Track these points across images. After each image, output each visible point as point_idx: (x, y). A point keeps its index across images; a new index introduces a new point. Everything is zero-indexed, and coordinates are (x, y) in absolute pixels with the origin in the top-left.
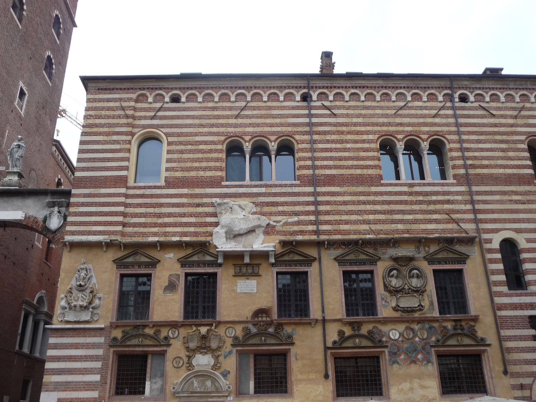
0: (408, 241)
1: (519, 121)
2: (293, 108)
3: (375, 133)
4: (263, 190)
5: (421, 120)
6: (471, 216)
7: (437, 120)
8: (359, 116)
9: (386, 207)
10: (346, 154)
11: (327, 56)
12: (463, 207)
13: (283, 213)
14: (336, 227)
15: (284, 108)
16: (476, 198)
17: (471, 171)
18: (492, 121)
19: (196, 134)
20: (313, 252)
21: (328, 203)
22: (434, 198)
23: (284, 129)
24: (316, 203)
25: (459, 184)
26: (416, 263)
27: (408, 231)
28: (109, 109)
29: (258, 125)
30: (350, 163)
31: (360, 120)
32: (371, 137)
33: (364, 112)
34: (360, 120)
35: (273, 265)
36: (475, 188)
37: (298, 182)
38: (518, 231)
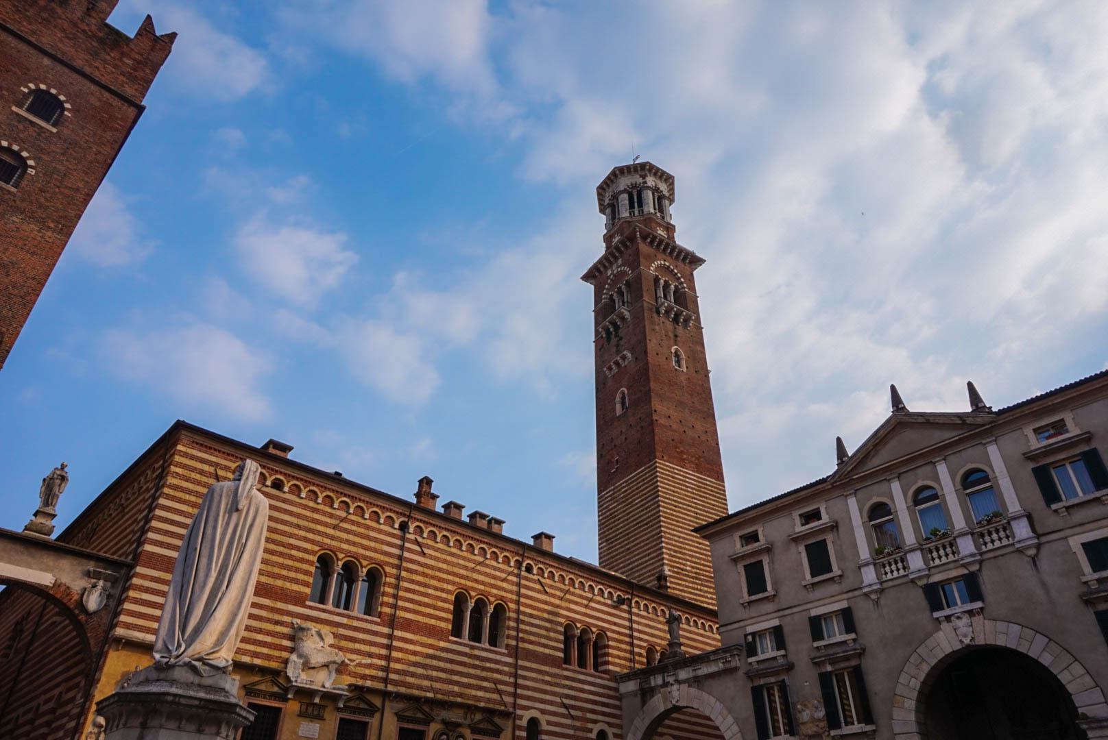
0: (460, 705)
1: (564, 604)
2: (390, 535)
3: (453, 583)
4: (345, 621)
5: (493, 581)
6: (511, 689)
7: (505, 585)
8: (445, 561)
9: (448, 666)
10: (426, 600)
11: (426, 482)
12: (506, 679)
13: (358, 652)
14: (402, 678)
15: (381, 531)
16: (520, 672)
17: (521, 645)
18: (544, 597)
19: (291, 536)
20: (377, 702)
21: (400, 650)
22: (488, 665)
23: (377, 556)
24: (389, 647)
25: (508, 655)
26: (461, 730)
27: (461, 695)
28: (202, 472)
29: (354, 544)
30: (428, 610)
31: (444, 566)
32: (450, 587)
33: (449, 558)
34: (444, 566)
35: (338, 709)
36: (520, 662)
37: (378, 620)
38: (543, 712)
